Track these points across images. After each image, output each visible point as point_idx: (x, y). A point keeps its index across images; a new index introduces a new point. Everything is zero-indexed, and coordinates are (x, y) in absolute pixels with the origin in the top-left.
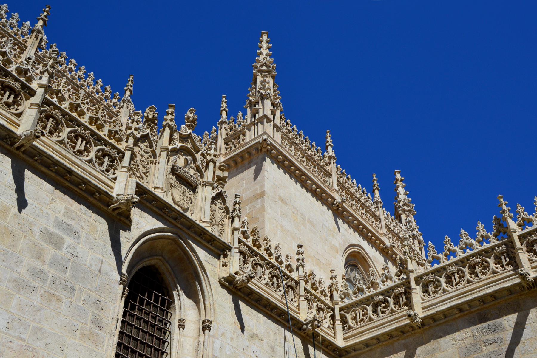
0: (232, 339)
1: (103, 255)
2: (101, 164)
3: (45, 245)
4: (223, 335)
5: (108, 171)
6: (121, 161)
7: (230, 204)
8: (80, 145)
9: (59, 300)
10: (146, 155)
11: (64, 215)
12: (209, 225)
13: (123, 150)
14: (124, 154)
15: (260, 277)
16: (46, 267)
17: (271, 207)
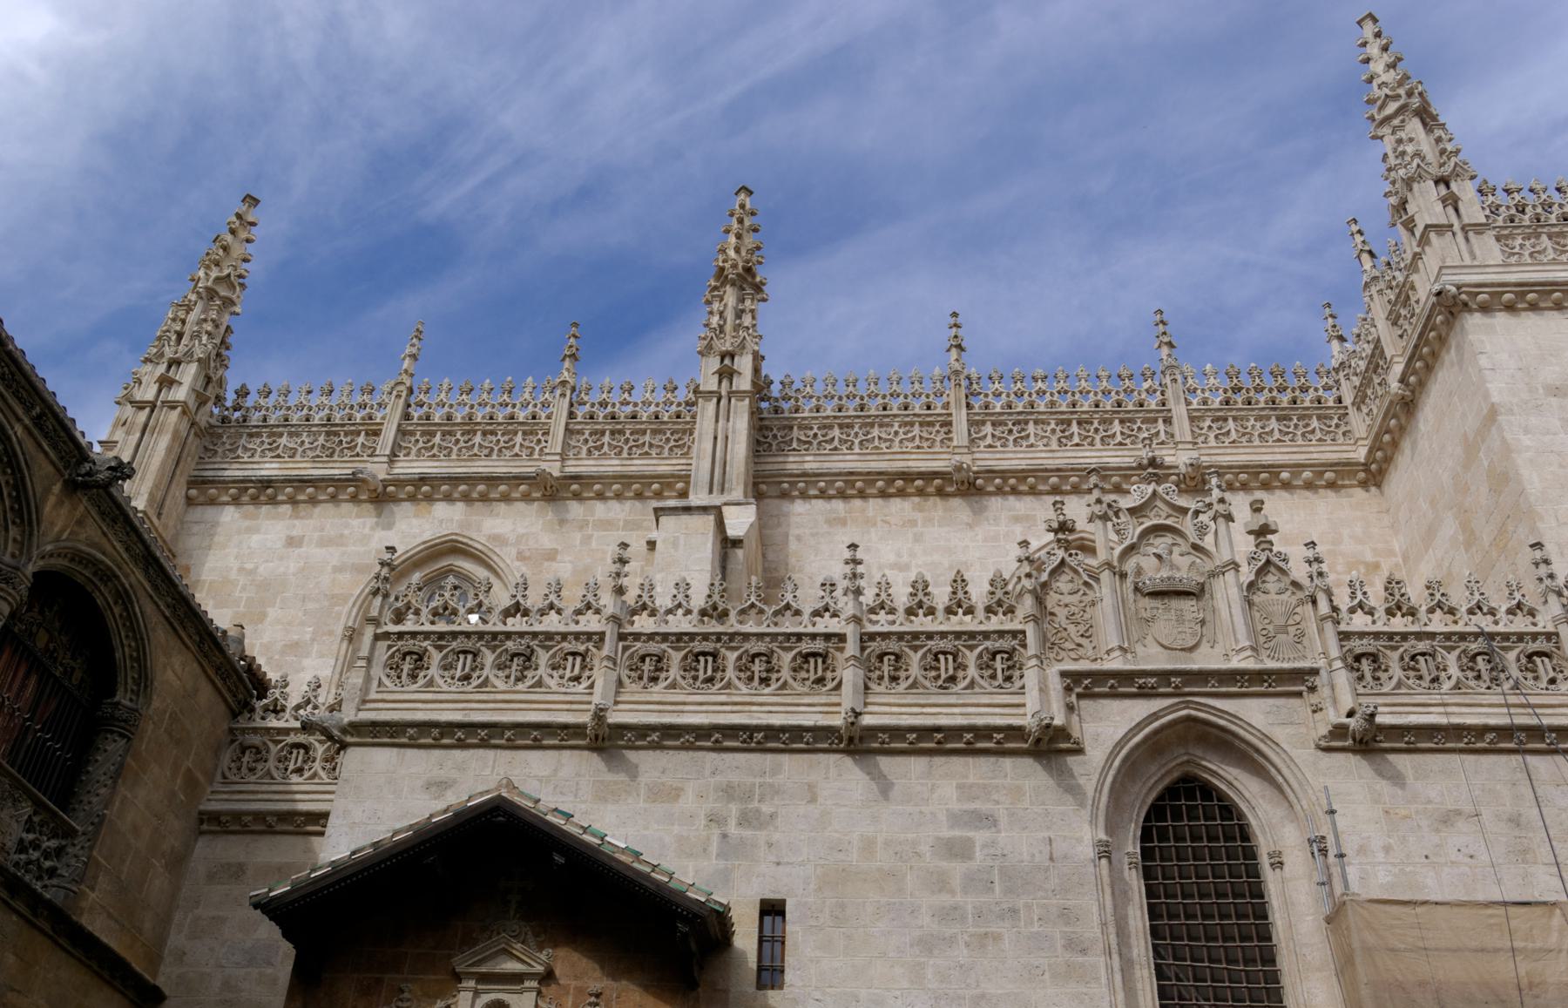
0: (1387, 849)
1: (1048, 828)
2: (993, 677)
3: (944, 864)
4: (1362, 850)
5: (1008, 679)
6: (1024, 646)
7: (1299, 571)
8: (946, 667)
9: (997, 938)
10: (1075, 599)
11: (959, 800)
12: (1249, 653)
13: (1020, 627)
14: (1024, 632)
15: (1435, 680)
16: (958, 898)
17: (1526, 431)
